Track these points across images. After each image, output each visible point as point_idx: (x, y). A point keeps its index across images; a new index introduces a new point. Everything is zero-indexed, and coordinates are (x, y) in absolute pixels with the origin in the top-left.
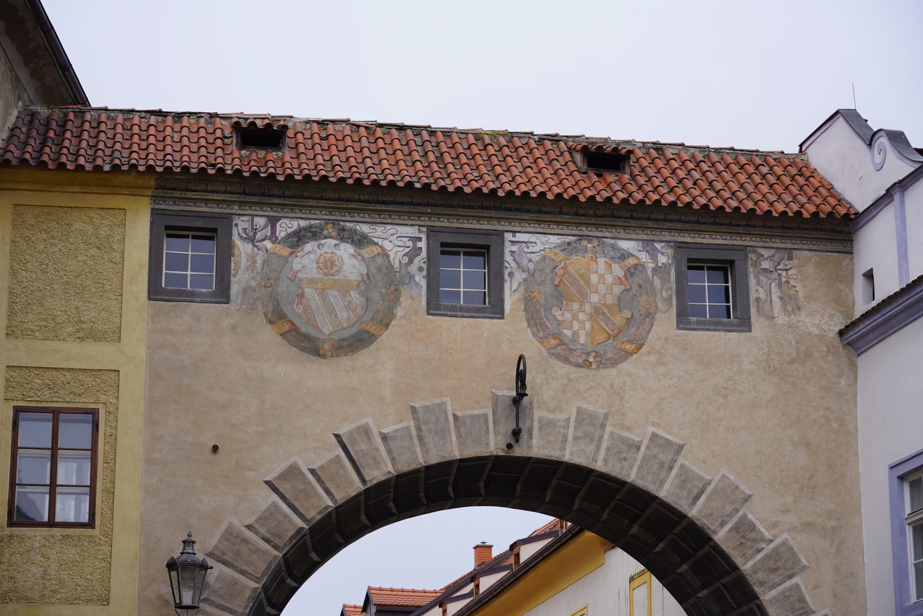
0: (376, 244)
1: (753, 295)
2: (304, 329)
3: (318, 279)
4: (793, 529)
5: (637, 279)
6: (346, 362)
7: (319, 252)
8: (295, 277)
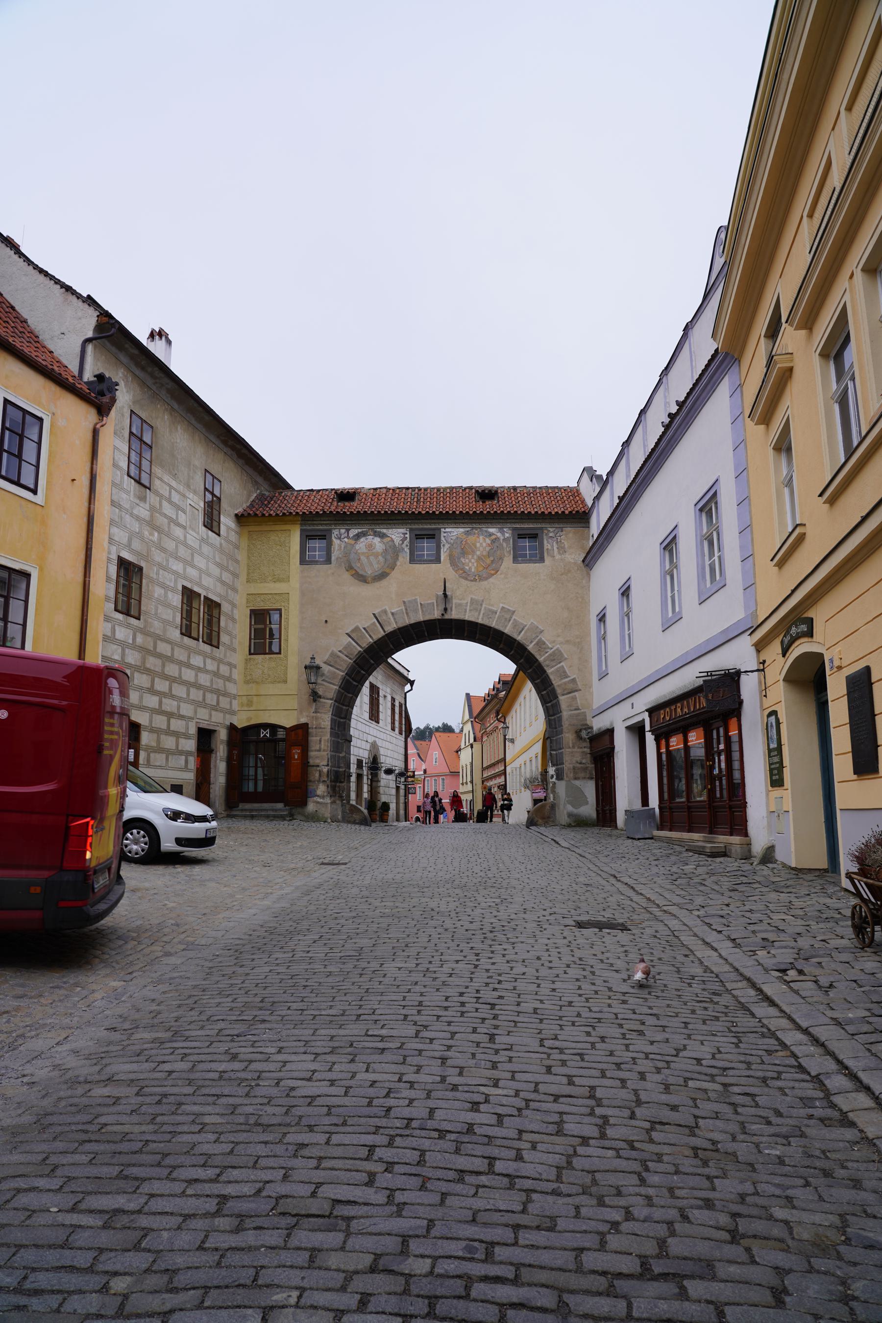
1: (545, 548)
2: (361, 572)
4: (561, 643)
5: (497, 544)
6: (377, 584)
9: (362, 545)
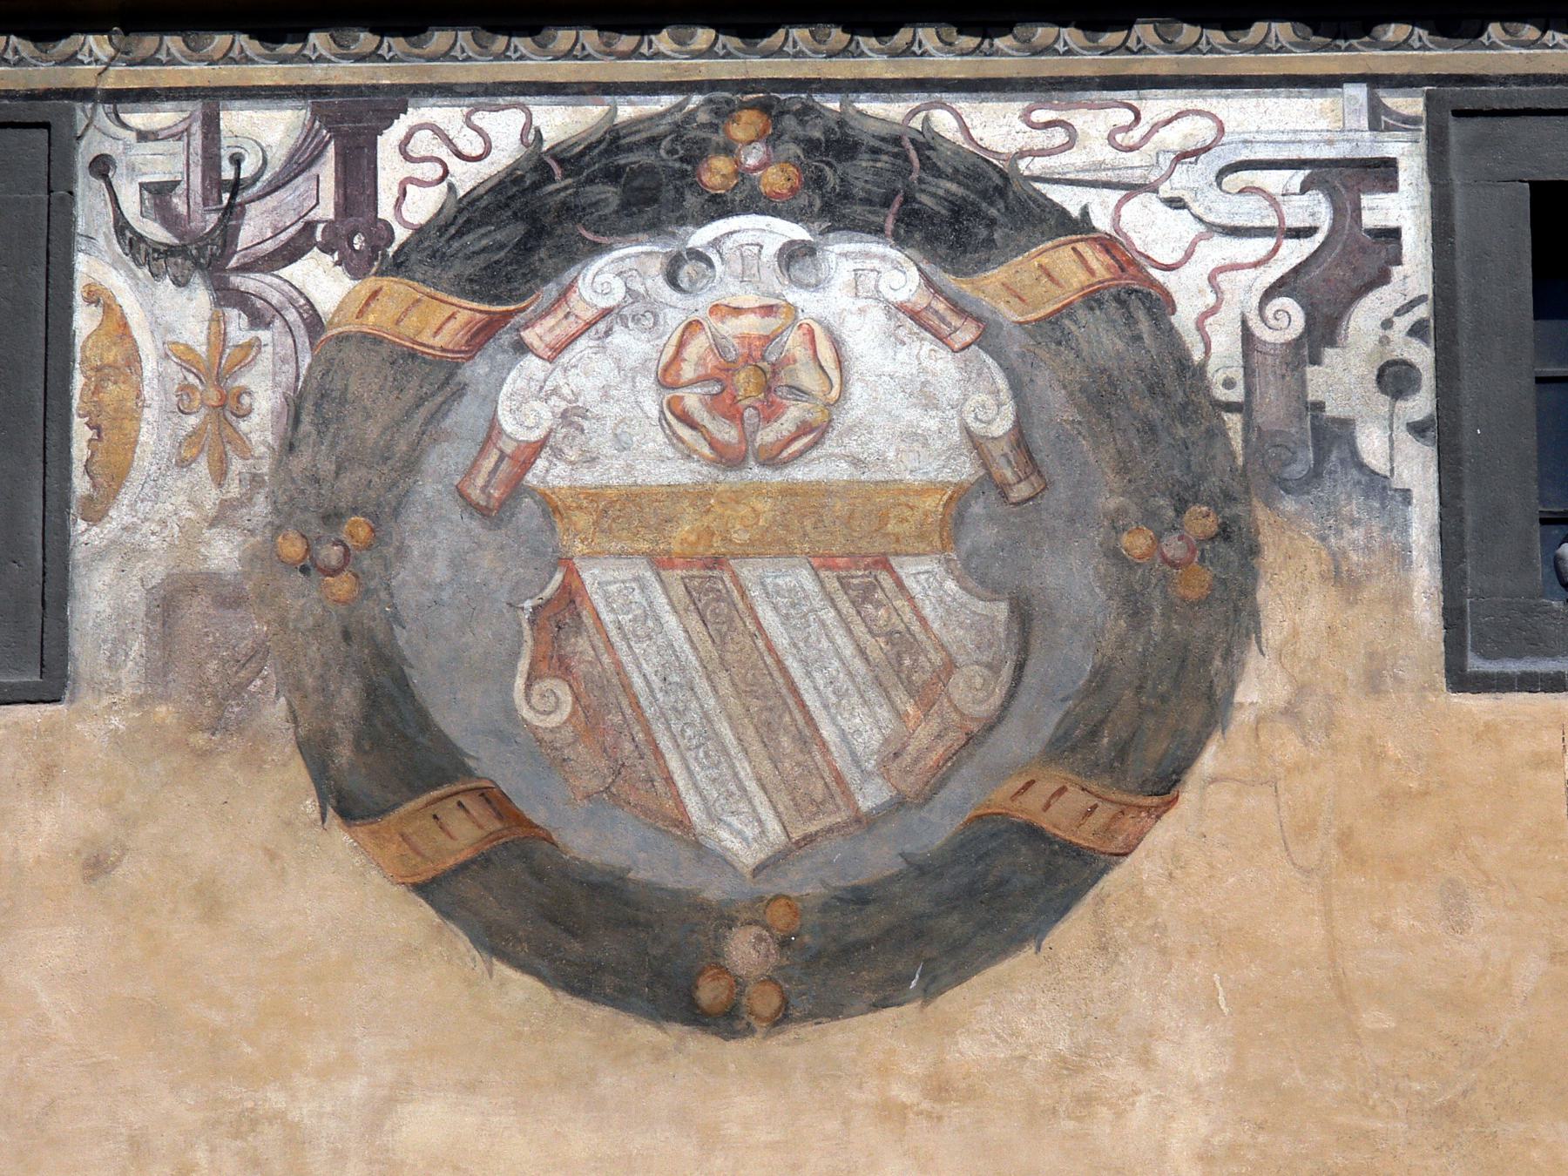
0: (1080, 226)
2: (588, 842)
3: (674, 493)
6: (879, 1047)
7: (676, 310)
8: (516, 488)
9: (594, 376)
